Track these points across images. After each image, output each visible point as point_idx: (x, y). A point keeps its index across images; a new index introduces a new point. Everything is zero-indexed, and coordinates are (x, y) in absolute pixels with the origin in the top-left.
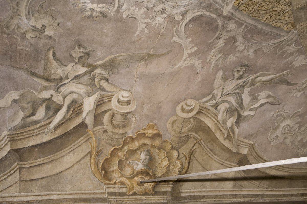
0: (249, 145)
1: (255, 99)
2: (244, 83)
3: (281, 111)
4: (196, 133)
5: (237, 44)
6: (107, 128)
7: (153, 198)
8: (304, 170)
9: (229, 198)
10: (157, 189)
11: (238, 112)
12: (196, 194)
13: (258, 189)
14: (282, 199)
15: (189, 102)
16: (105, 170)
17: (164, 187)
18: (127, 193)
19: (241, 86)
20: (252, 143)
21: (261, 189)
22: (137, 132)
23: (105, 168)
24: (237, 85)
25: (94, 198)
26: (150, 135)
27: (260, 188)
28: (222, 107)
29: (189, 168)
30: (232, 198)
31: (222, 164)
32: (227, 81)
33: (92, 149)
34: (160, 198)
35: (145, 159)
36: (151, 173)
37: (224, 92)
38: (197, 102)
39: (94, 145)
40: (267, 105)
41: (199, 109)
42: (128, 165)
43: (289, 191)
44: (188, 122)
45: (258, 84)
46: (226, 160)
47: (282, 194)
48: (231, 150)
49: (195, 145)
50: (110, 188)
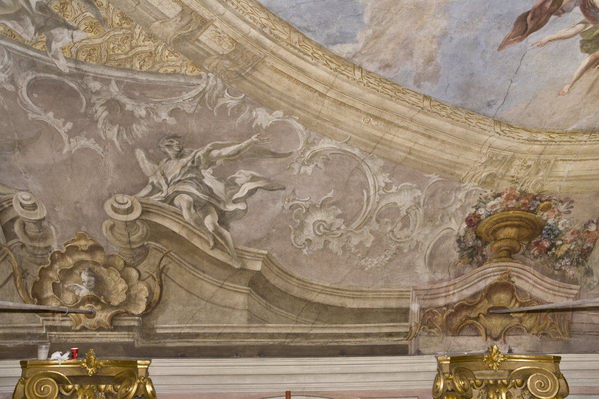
0: (262, 256)
1: (232, 185)
2: (193, 162)
3: (294, 200)
4: (156, 242)
5: (129, 107)
6: (24, 242)
7: (112, 335)
8: (384, 293)
9: (244, 338)
10: (116, 323)
11: (216, 207)
12: (182, 332)
13: (296, 325)
14: (346, 342)
15: (119, 198)
16: (37, 296)
17: (127, 320)
18: (73, 328)
19: (192, 167)
20: (266, 252)
21: (303, 325)
22: (65, 245)
23: (37, 294)
24: (183, 167)
25: (30, 333)
26: (86, 248)
27: (300, 323)
28: (182, 201)
29: (164, 292)
30: (248, 338)
31: (221, 287)
32: (162, 163)
33: (14, 270)
34: (123, 336)
35: (89, 282)
36: (103, 301)
37: (169, 179)
38: (133, 198)
39: (16, 265)
40: (259, 192)
41: (143, 207)
42: (67, 289)
43: (360, 327)
44: (135, 228)
45: (219, 162)
46: (225, 280)
47: (346, 334)
48: (229, 266)
49: (162, 259)
50: (48, 320)
